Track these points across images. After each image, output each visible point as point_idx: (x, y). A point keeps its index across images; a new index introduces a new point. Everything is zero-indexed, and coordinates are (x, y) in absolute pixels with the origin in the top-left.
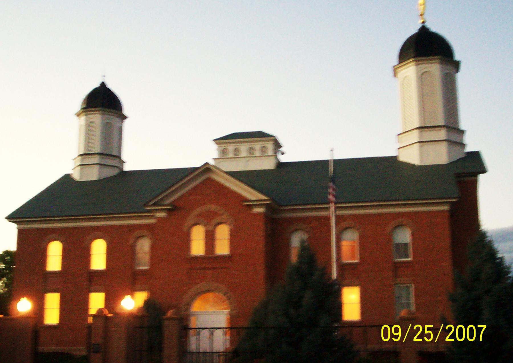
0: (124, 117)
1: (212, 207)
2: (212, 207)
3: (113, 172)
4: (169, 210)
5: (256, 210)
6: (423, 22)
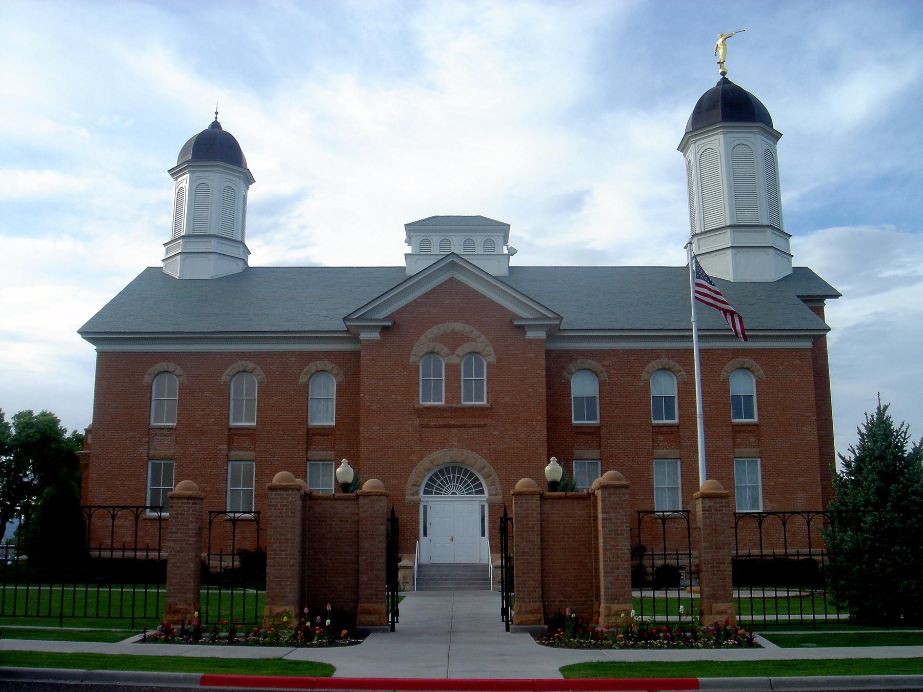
0: (777, 136)
1: (458, 326)
2: (458, 326)
3: (237, 268)
4: (385, 329)
5: (530, 335)
6: (723, 74)
